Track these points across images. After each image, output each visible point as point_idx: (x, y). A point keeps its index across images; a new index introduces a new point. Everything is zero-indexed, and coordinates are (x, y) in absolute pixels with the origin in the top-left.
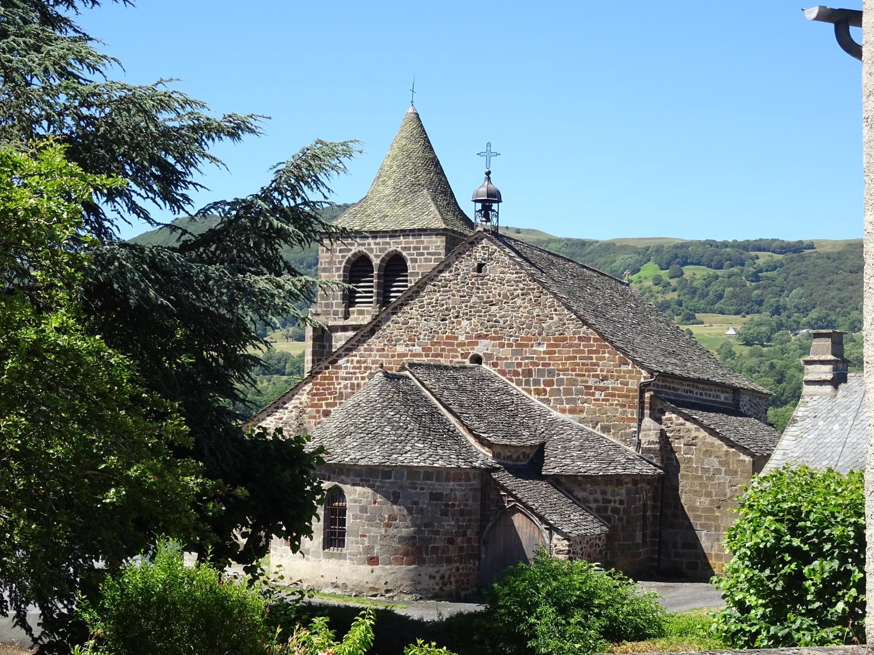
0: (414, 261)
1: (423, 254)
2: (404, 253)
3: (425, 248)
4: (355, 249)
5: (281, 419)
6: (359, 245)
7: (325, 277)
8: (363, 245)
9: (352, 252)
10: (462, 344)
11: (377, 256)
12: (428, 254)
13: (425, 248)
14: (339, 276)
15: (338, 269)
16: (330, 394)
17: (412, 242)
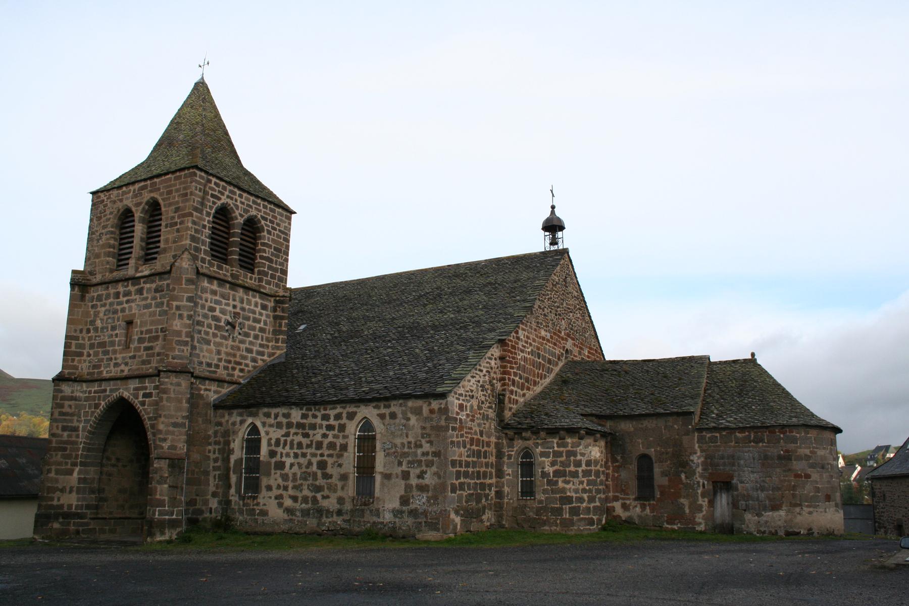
0: (269, 232)
1: (275, 229)
2: (263, 222)
3: (278, 225)
4: (224, 199)
5: (479, 381)
6: (228, 197)
7: (197, 217)
8: (232, 199)
9: (222, 201)
10: (563, 339)
11: (241, 216)
12: (280, 231)
13: (278, 225)
14: (209, 222)
15: (208, 214)
16: (516, 363)
17: (269, 215)
